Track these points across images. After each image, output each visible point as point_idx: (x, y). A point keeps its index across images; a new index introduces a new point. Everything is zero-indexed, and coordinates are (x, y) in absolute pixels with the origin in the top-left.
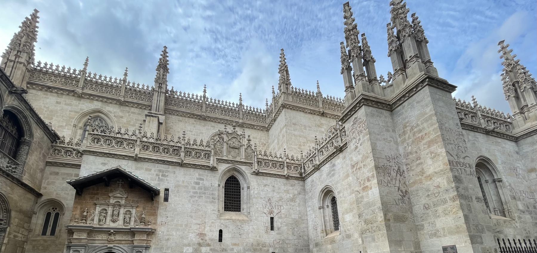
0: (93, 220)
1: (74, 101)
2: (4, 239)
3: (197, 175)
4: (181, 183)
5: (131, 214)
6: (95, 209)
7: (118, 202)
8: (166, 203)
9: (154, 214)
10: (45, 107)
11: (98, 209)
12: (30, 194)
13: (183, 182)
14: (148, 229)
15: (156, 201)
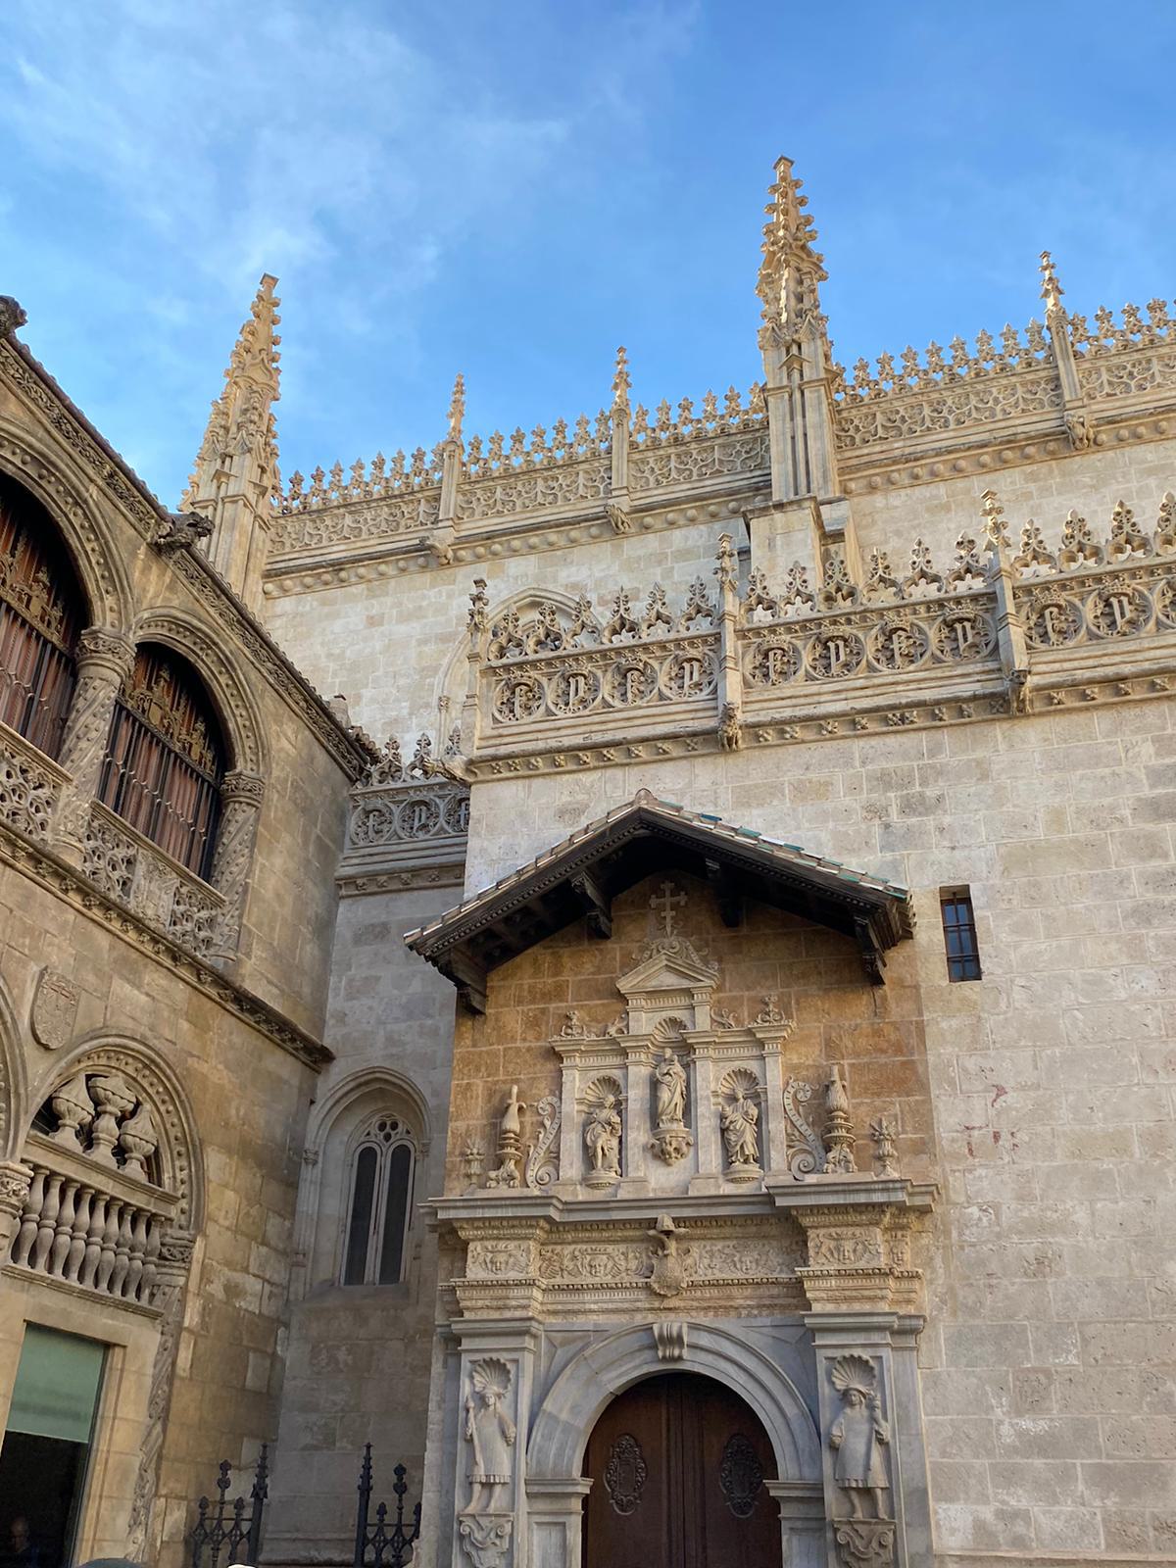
0: (554, 1158)
1: (432, 593)
2: (183, 1302)
3: (1147, 749)
4: (1041, 832)
5: (757, 1097)
6: (558, 1088)
7: (675, 1023)
8: (969, 988)
9: (901, 1073)
10: (329, 655)
11: (578, 1083)
12: (280, 1054)
13: (1057, 818)
14: (887, 1186)
15: (900, 983)
